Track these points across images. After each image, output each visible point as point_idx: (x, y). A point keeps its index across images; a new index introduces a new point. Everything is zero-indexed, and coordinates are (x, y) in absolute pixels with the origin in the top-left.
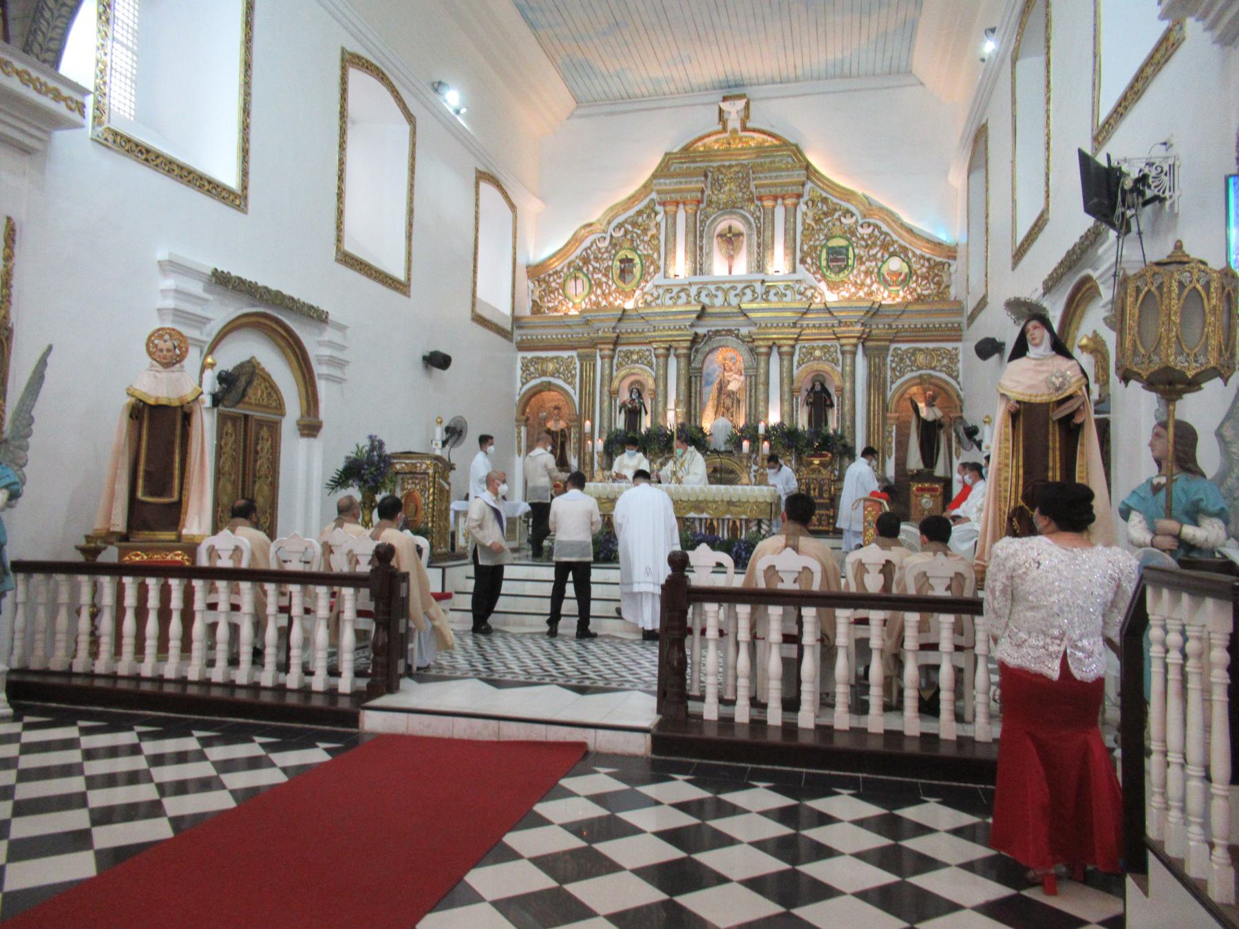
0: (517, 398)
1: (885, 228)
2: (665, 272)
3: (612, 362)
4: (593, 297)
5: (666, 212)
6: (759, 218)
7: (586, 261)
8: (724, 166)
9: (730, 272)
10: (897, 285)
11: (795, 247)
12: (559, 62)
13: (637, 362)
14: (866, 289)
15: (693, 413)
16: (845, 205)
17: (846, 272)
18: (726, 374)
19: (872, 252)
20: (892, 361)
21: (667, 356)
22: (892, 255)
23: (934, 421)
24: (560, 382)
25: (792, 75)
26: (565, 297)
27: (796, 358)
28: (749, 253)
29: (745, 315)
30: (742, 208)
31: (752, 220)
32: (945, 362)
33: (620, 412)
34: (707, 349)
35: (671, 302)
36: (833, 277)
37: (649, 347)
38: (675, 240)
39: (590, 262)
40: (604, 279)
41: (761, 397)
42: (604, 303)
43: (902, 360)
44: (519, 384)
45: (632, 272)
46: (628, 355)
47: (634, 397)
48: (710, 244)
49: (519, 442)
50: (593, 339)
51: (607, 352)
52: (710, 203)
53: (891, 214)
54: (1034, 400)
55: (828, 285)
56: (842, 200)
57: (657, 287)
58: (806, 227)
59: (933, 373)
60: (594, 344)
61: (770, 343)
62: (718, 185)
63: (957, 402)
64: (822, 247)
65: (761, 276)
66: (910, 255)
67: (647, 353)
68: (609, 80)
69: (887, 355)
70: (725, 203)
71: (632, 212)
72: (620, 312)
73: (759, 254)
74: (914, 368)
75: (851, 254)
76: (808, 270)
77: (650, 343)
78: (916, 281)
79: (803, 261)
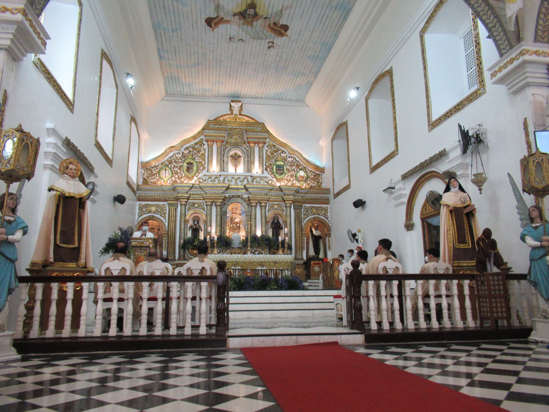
0: (136, 223)
1: (297, 159)
4: (174, 179)
5: (208, 145)
6: (248, 151)
7: (170, 162)
8: (233, 128)
9: (236, 171)
12: (166, 75)
13: (197, 207)
14: (291, 182)
16: (283, 149)
18: (233, 215)
19: (293, 168)
20: (304, 211)
21: (211, 205)
22: (300, 170)
23: (318, 236)
24: (158, 216)
25: (260, 96)
26: (160, 177)
27: (267, 208)
28: (244, 164)
30: (241, 146)
31: (245, 151)
32: (323, 212)
35: (211, 182)
36: (278, 176)
38: (212, 157)
39: (172, 163)
40: (179, 171)
42: (179, 181)
44: (137, 217)
47: (195, 223)
48: (228, 159)
50: (177, 197)
51: (183, 203)
52: (227, 143)
53: (300, 154)
54: (457, 206)
55: (277, 180)
56: (281, 146)
57: (205, 175)
58: (268, 156)
60: (177, 199)
61: (257, 202)
62: (230, 135)
64: (274, 164)
65: (250, 174)
66: (307, 170)
67: (202, 204)
68: (185, 87)
70: (233, 143)
71: (193, 143)
72: (192, 185)
73: (248, 165)
76: (268, 173)
77: (204, 199)
78: (310, 180)
79: (266, 170)
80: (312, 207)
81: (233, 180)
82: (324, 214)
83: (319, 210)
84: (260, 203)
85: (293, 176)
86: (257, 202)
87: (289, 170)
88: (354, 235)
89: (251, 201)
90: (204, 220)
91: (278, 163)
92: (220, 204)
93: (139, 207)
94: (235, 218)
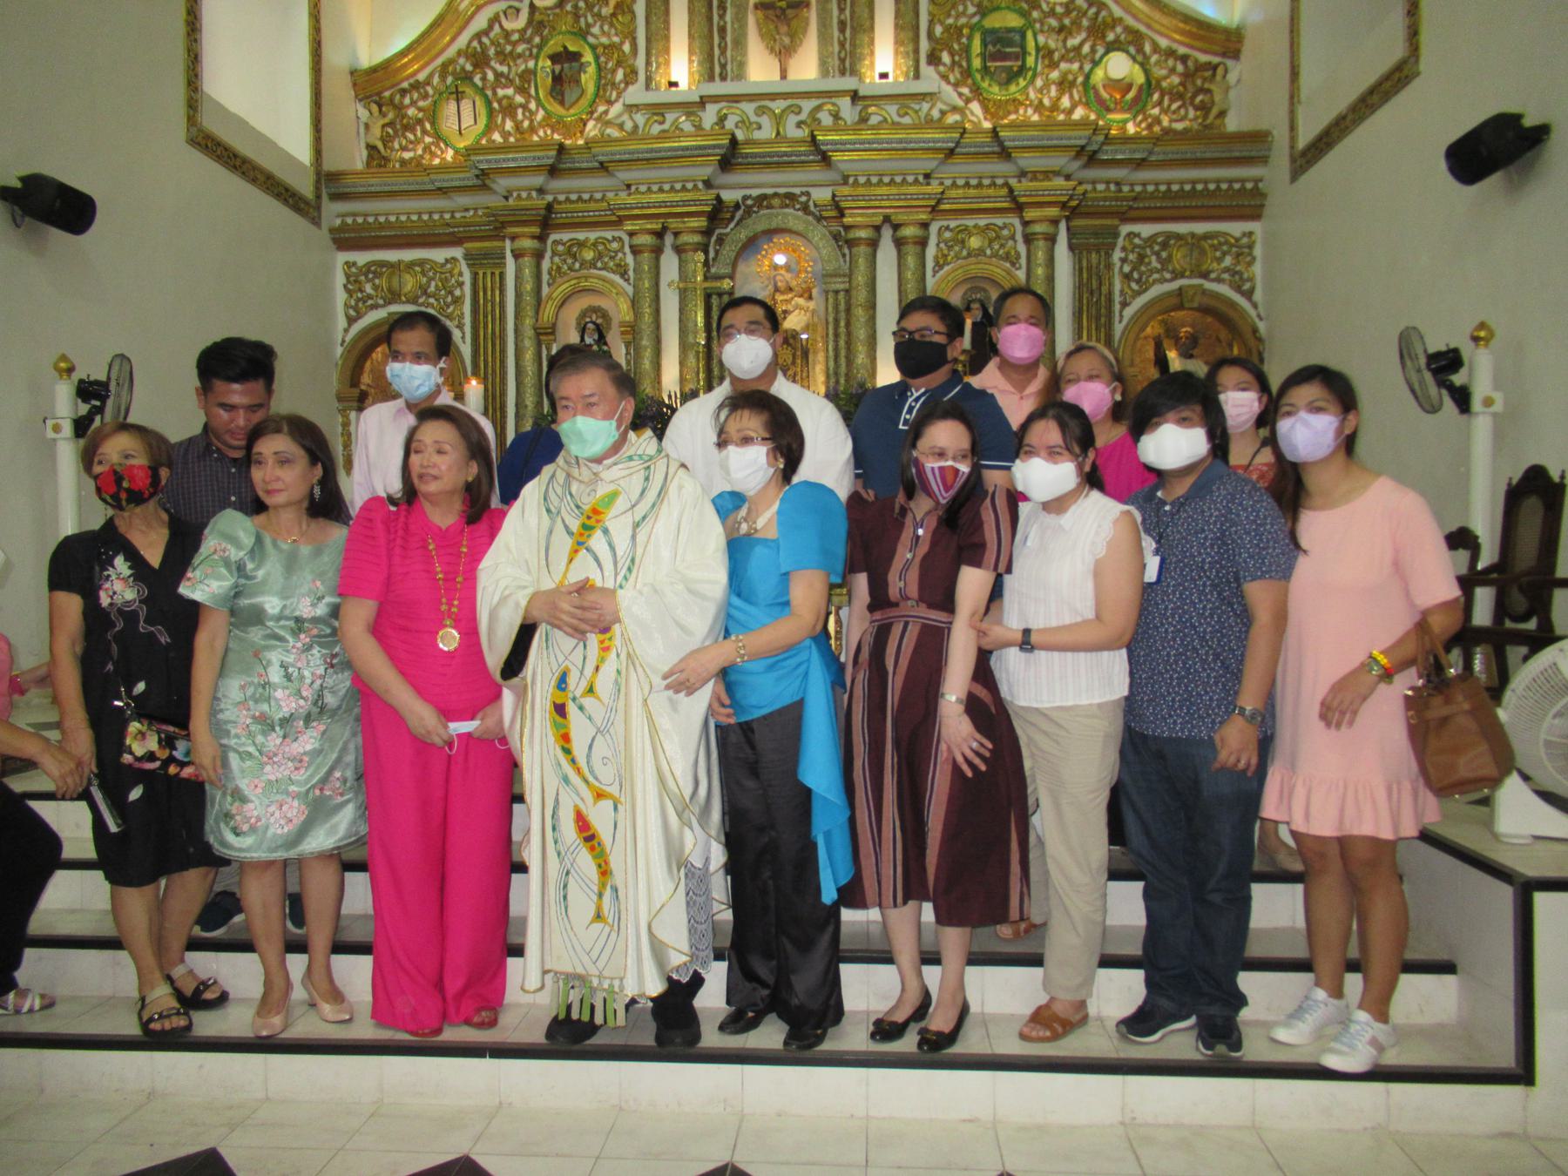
0: (339, 350)
2: (649, 80)
3: (538, 266)
4: (497, 137)
7: (480, 61)
9: (784, 76)
10: (1123, 111)
11: (918, 27)
13: (593, 265)
17: (1022, 83)
18: (779, 297)
19: (1072, 42)
20: (1124, 260)
21: (658, 251)
22: (1111, 47)
26: (438, 137)
27: (931, 251)
28: (824, 38)
29: (825, 159)
34: (743, 235)
36: (995, 92)
37: (617, 234)
38: (667, 12)
39: (487, 64)
40: (519, 99)
41: (861, 333)
43: (1141, 258)
44: (342, 322)
45: (578, 82)
47: (588, 340)
48: (741, 20)
55: (986, 110)
57: (631, 108)
59: (1208, 285)
60: (499, 225)
63: (1252, 342)
65: (848, 83)
66: (1148, 48)
67: (615, 245)
69: (1113, 247)
72: (554, 153)
73: (842, 45)
74: (1168, 276)
75: (1031, 45)
76: (944, 77)
77: (619, 222)
79: (933, 59)
80: (1170, 236)
81: (765, 121)
82: (1235, 273)
83: (1203, 252)
85: (1073, 84)
87: (1050, 53)
88: (1446, 363)
89: (847, 220)
90: (622, 324)
91: (995, 21)
92: (697, 238)
93: (348, 276)
94: (785, 312)
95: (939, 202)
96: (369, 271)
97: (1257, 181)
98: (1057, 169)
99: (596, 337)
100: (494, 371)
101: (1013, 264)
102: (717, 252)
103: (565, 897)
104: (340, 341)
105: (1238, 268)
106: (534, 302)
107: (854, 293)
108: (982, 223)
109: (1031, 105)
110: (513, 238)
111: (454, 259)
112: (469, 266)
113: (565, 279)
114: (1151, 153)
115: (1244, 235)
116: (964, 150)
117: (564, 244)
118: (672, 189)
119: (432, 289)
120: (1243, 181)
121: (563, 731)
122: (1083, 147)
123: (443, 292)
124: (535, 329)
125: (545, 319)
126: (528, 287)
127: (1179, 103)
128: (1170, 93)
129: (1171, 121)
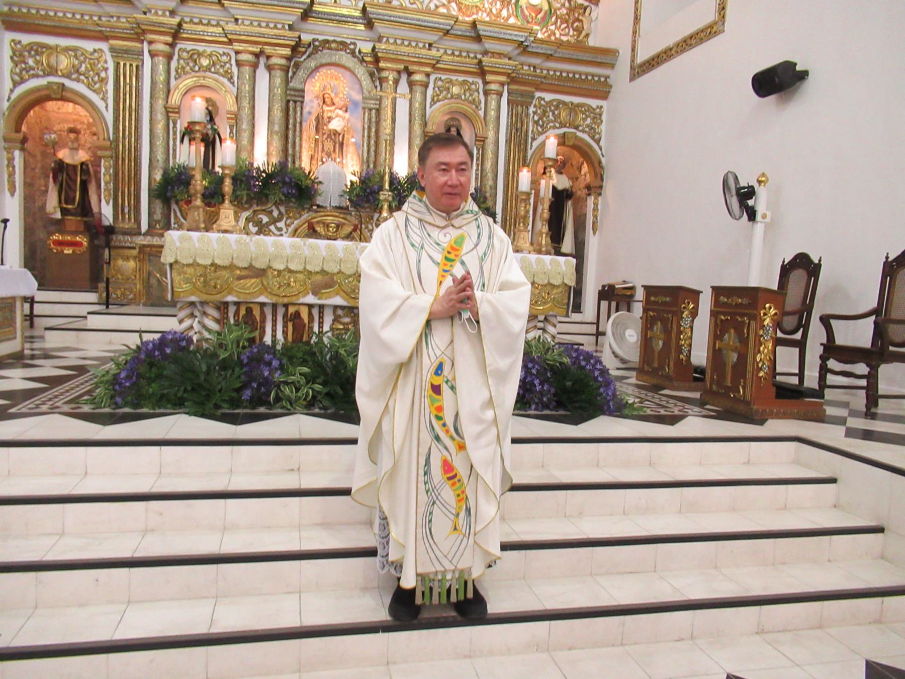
0: (6, 105)
3: (169, 64)
10: (536, 24)
13: (208, 69)
15: (290, 152)
18: (326, 108)
20: (535, 113)
21: (255, 66)
24: (81, 88)
27: (430, 92)
33: (182, 141)
43: (544, 112)
44: (9, 84)
46: (194, 57)
49: (11, 175)
55: (460, 9)
61: (401, 67)
63: (598, 169)
67: (224, 58)
74: (557, 125)
77: (231, 42)
78: (556, 23)
80: (560, 102)
82: (591, 128)
83: (576, 114)
84: (410, 74)
86: (401, 67)
89: (382, 64)
90: (229, 112)
92: (283, 62)
93: (14, 51)
94: (330, 119)
95: (438, 62)
96: (32, 49)
97: (607, 77)
98: (506, 53)
99: (208, 118)
100: (130, 133)
101: (477, 107)
102: (294, 73)
103: (430, 521)
104: (7, 97)
105: (593, 126)
106: (165, 90)
107: (383, 112)
108: (461, 79)
109: (485, 11)
110: (150, 43)
111: (100, 50)
112: (112, 56)
113: (188, 76)
114: (555, 52)
115: (598, 107)
116: (454, 32)
117: (188, 52)
118: (267, 26)
119: (83, 69)
120: (599, 76)
121: (436, 404)
122: (522, 42)
123: (91, 73)
124: (166, 108)
125: (173, 102)
126: (162, 79)
127: (565, 25)
128: (561, 18)
129: (561, 35)
